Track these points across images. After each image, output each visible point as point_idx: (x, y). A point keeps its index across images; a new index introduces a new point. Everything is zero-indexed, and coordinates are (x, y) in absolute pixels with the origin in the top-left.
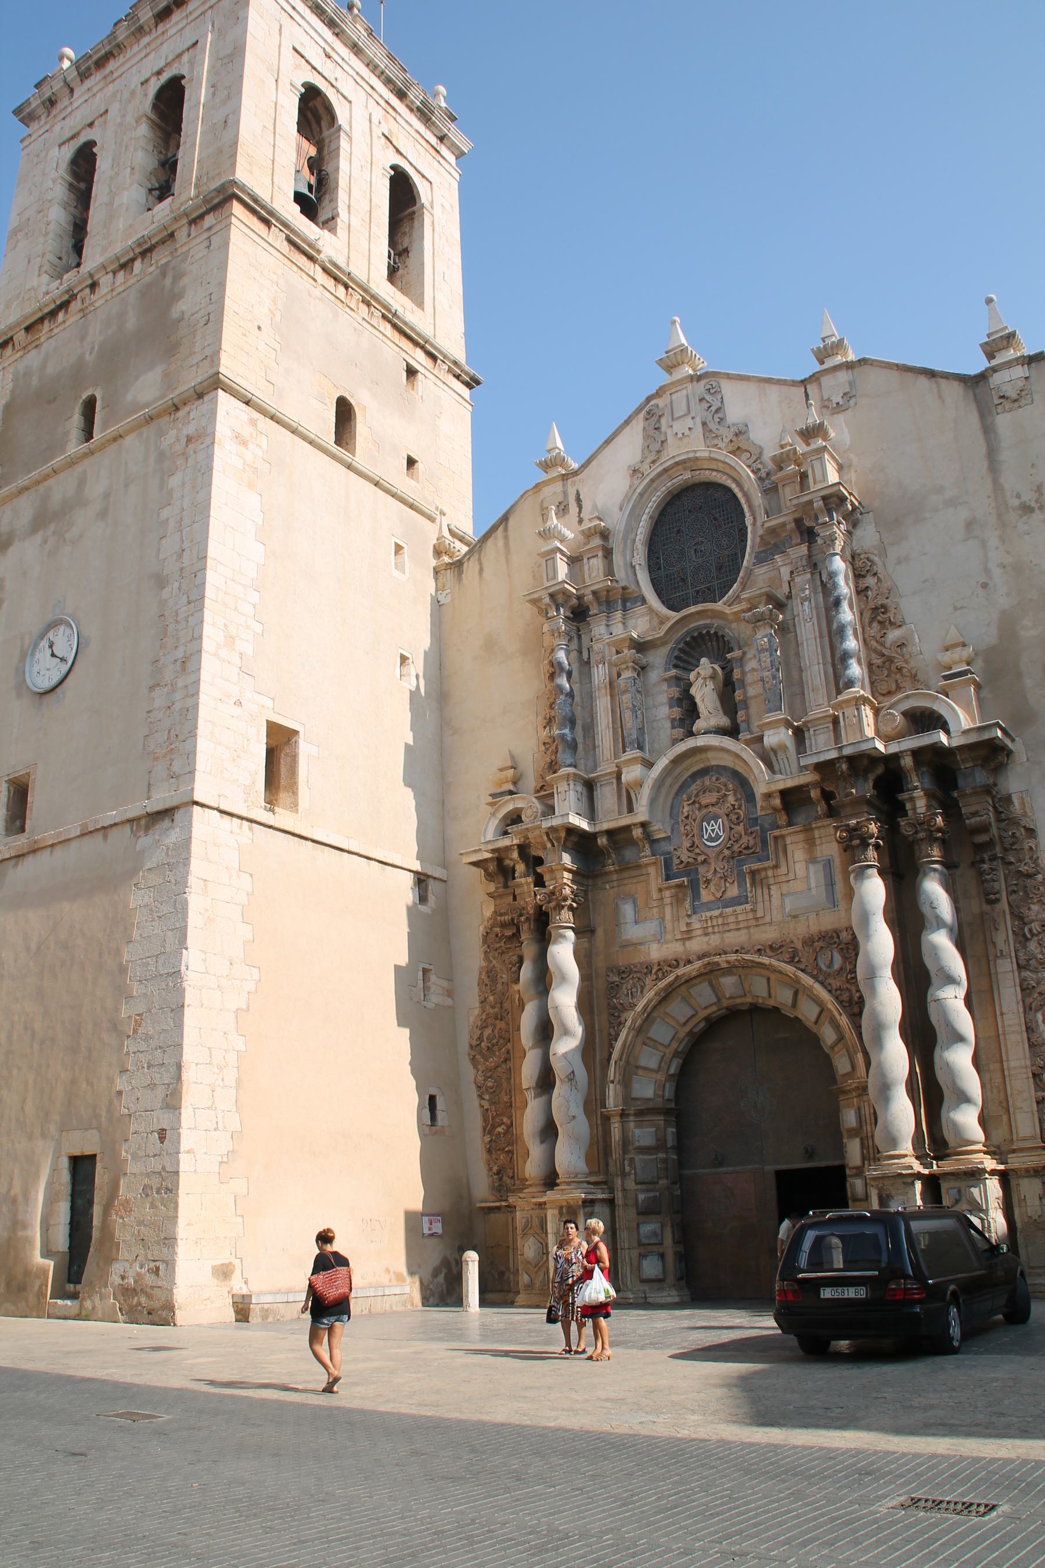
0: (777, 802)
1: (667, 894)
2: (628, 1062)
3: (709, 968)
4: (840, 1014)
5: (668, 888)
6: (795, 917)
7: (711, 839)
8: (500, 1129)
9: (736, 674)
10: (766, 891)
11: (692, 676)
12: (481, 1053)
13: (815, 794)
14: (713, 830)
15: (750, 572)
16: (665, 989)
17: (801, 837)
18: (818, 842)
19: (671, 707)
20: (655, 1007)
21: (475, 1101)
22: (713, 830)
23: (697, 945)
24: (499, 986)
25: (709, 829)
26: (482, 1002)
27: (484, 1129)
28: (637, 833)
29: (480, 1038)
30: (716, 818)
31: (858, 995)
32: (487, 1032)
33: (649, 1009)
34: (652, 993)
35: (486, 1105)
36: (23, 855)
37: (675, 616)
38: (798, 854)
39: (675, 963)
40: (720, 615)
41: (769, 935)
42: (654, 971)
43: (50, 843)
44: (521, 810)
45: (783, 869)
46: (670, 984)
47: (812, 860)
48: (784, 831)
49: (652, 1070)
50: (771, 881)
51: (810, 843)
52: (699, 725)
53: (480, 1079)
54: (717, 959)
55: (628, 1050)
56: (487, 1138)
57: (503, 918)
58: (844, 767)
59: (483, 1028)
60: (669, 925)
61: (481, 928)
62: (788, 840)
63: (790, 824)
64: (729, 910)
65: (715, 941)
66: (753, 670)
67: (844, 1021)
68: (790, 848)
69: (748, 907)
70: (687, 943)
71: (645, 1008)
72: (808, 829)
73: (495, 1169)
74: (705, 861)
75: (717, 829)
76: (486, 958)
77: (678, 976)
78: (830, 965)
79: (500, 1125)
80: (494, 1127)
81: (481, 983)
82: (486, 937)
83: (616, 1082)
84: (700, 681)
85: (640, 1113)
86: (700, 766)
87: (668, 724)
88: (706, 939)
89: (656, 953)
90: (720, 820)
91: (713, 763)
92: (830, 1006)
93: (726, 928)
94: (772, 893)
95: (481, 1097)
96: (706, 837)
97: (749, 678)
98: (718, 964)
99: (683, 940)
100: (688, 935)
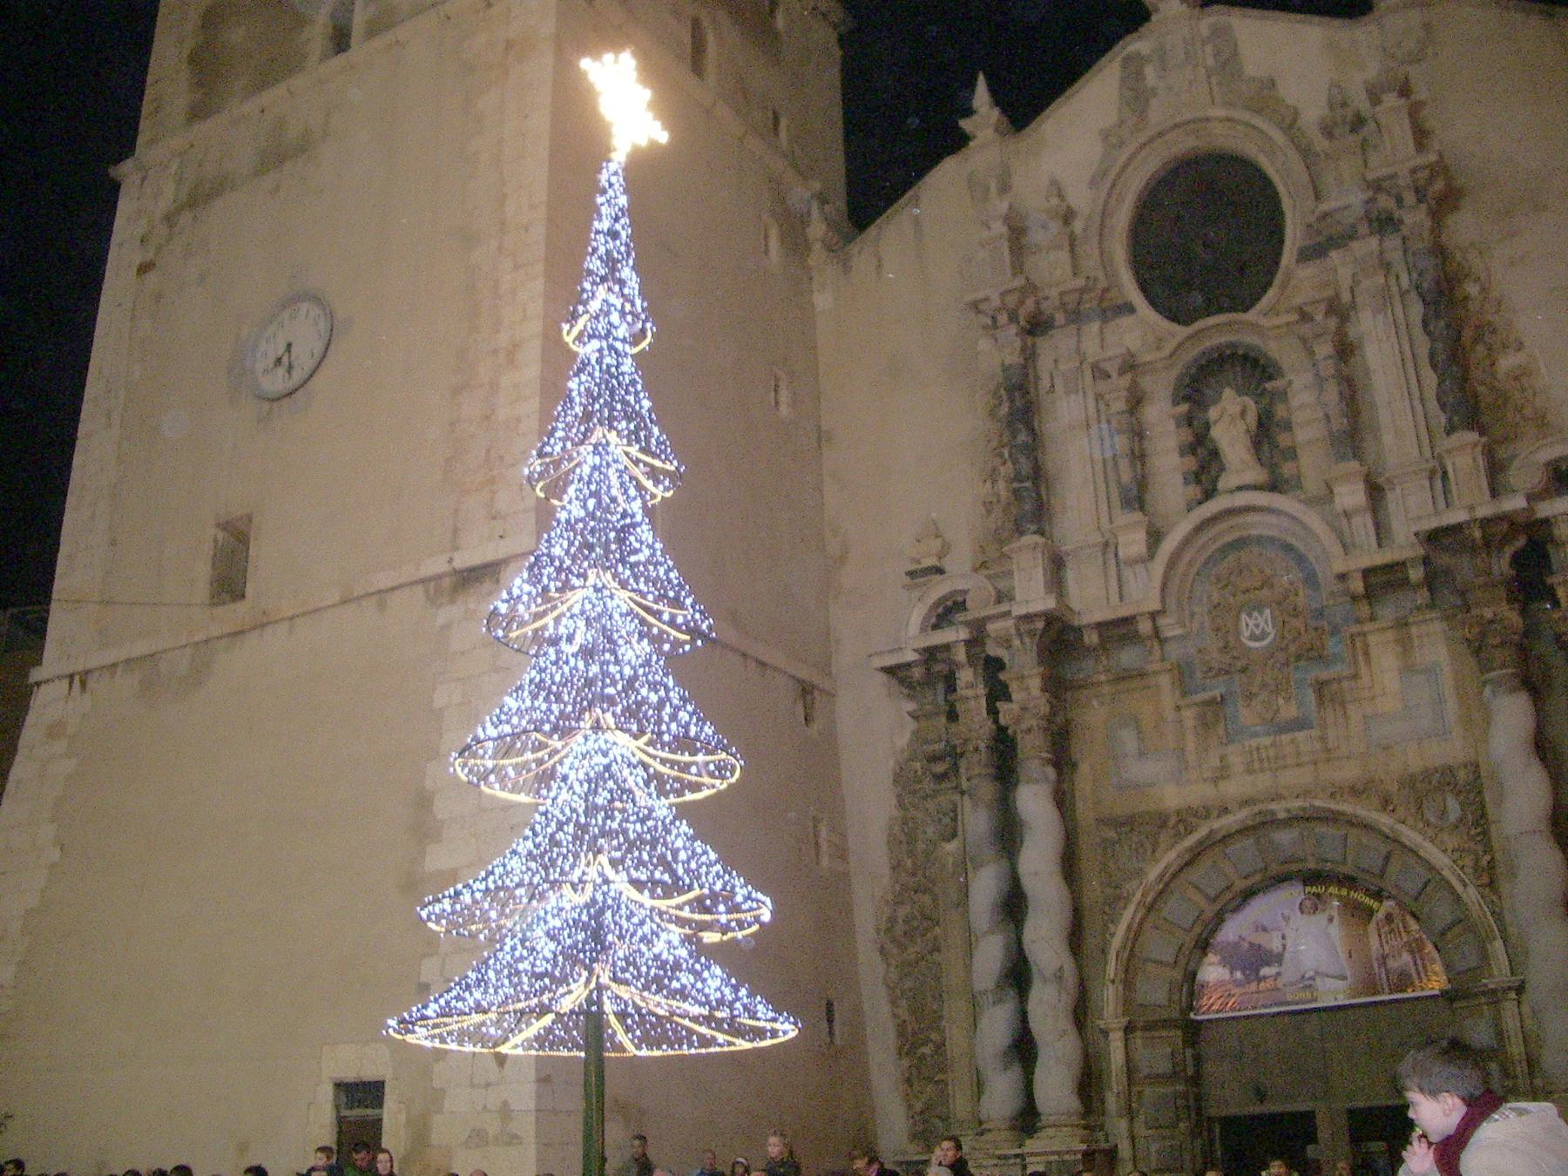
0: (1358, 586)
1: (1189, 715)
2: (1132, 954)
3: (1258, 819)
4: (1465, 885)
5: (1188, 706)
6: (1386, 748)
7: (1254, 638)
8: (927, 1050)
9: (1280, 411)
10: (1340, 712)
11: (1213, 413)
12: (894, 940)
13: (1416, 574)
14: (1257, 626)
15: (1288, 277)
16: (1191, 849)
17: (1390, 635)
18: (1416, 642)
19: (1182, 455)
20: (1175, 876)
21: (885, 1009)
22: (1257, 626)
23: (1234, 788)
24: (921, 846)
25: (1251, 623)
26: (893, 869)
27: (900, 1049)
28: (1145, 627)
29: (892, 920)
30: (1259, 607)
31: (1488, 857)
32: (903, 912)
33: (1166, 878)
34: (1172, 855)
35: (905, 1015)
36: (242, 632)
37: (1182, 332)
38: (1385, 659)
39: (1204, 813)
40: (1255, 328)
41: (1348, 772)
42: (1172, 822)
43: (290, 614)
44: (965, 592)
45: (1365, 681)
46: (1200, 842)
47: (1408, 669)
48: (1368, 627)
49: (1167, 965)
50: (1348, 697)
51: (1405, 645)
52: (1226, 481)
53: (894, 976)
54: (1273, 806)
55: (1135, 934)
56: (905, 1062)
57: (932, 748)
58: (1477, 534)
59: (898, 903)
60: (1191, 757)
61: (891, 763)
62: (1372, 639)
63: (1372, 618)
64: (1285, 738)
65: (1263, 782)
66: (1302, 406)
67: (1471, 895)
68: (1374, 652)
69: (1315, 733)
70: (1222, 785)
71: (1162, 875)
72: (1402, 624)
73: (918, 1106)
74: (1244, 670)
75: (1262, 624)
76: (901, 804)
77: (1211, 831)
78: (1443, 813)
79: (925, 1044)
80: (914, 1047)
81: (893, 841)
82: (898, 778)
83: (1117, 981)
84: (1226, 419)
85: (1149, 1027)
86: (1235, 535)
87: (1179, 479)
88: (1250, 778)
89: (1172, 798)
90: (1267, 612)
91: (1255, 532)
92: (1446, 873)
93: (1281, 762)
94: (1350, 713)
95: (894, 1002)
96: (1246, 634)
97: (1298, 418)
98: (1273, 813)
99: (1215, 781)
100: (1222, 773)
